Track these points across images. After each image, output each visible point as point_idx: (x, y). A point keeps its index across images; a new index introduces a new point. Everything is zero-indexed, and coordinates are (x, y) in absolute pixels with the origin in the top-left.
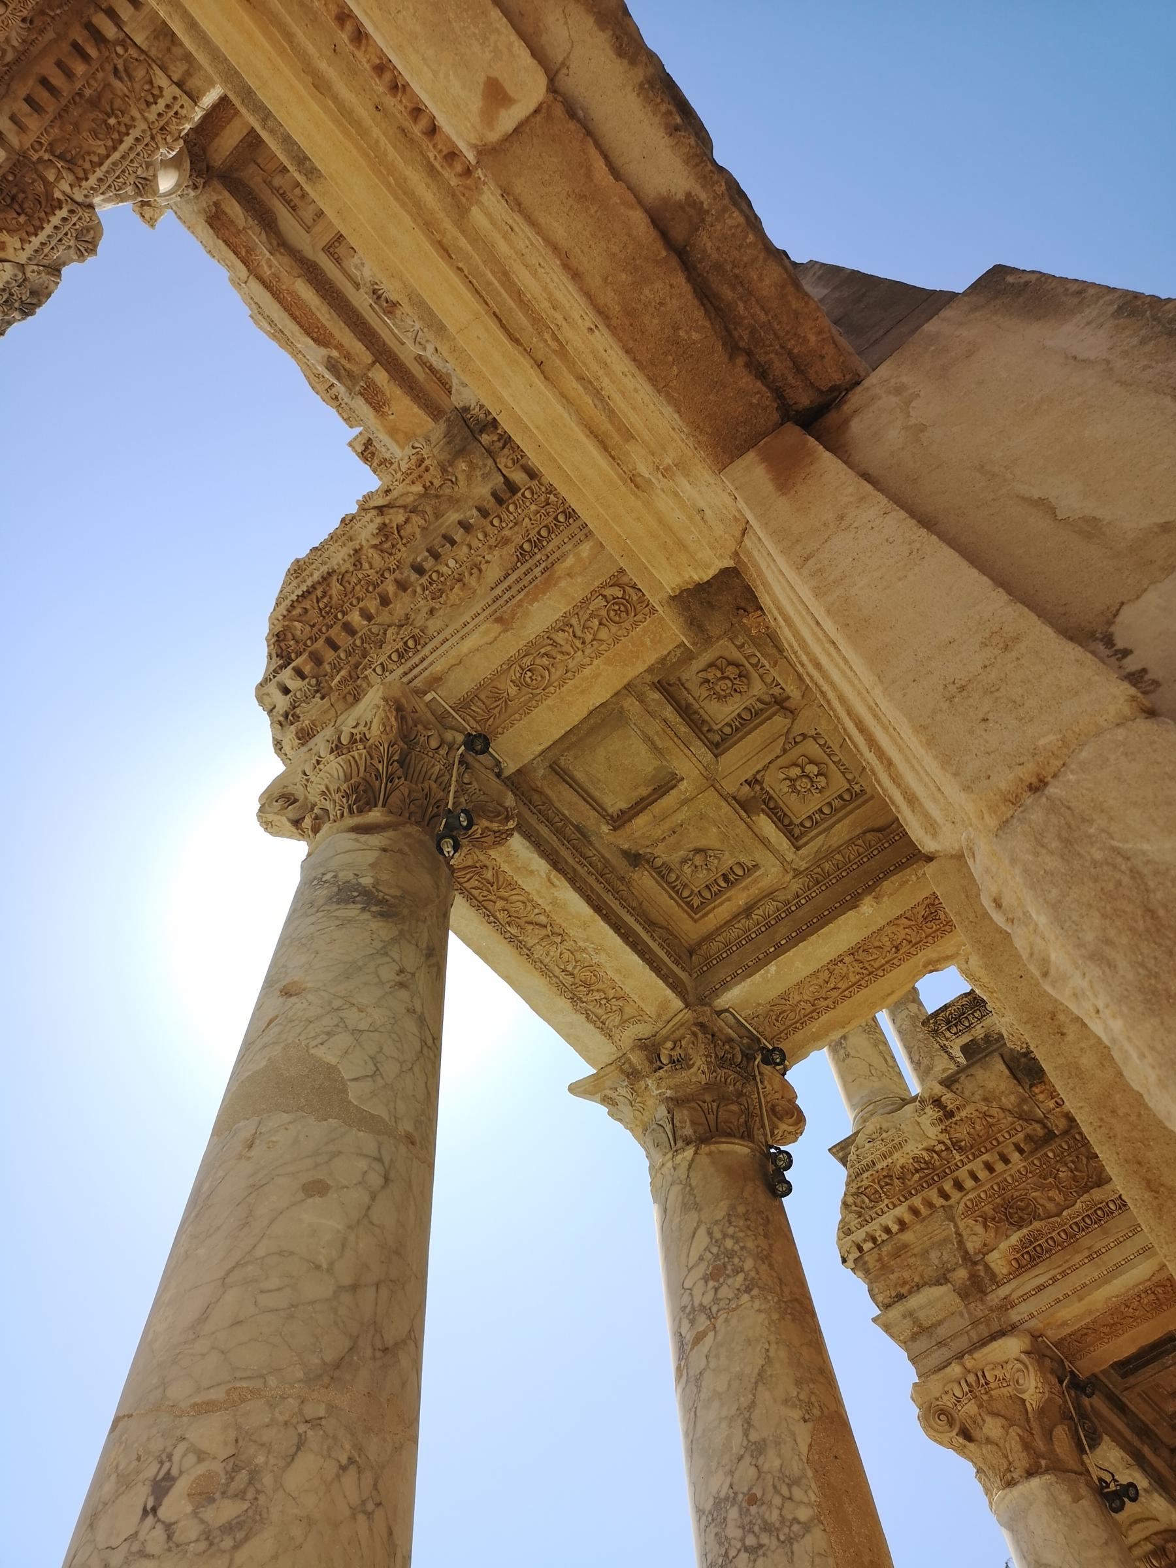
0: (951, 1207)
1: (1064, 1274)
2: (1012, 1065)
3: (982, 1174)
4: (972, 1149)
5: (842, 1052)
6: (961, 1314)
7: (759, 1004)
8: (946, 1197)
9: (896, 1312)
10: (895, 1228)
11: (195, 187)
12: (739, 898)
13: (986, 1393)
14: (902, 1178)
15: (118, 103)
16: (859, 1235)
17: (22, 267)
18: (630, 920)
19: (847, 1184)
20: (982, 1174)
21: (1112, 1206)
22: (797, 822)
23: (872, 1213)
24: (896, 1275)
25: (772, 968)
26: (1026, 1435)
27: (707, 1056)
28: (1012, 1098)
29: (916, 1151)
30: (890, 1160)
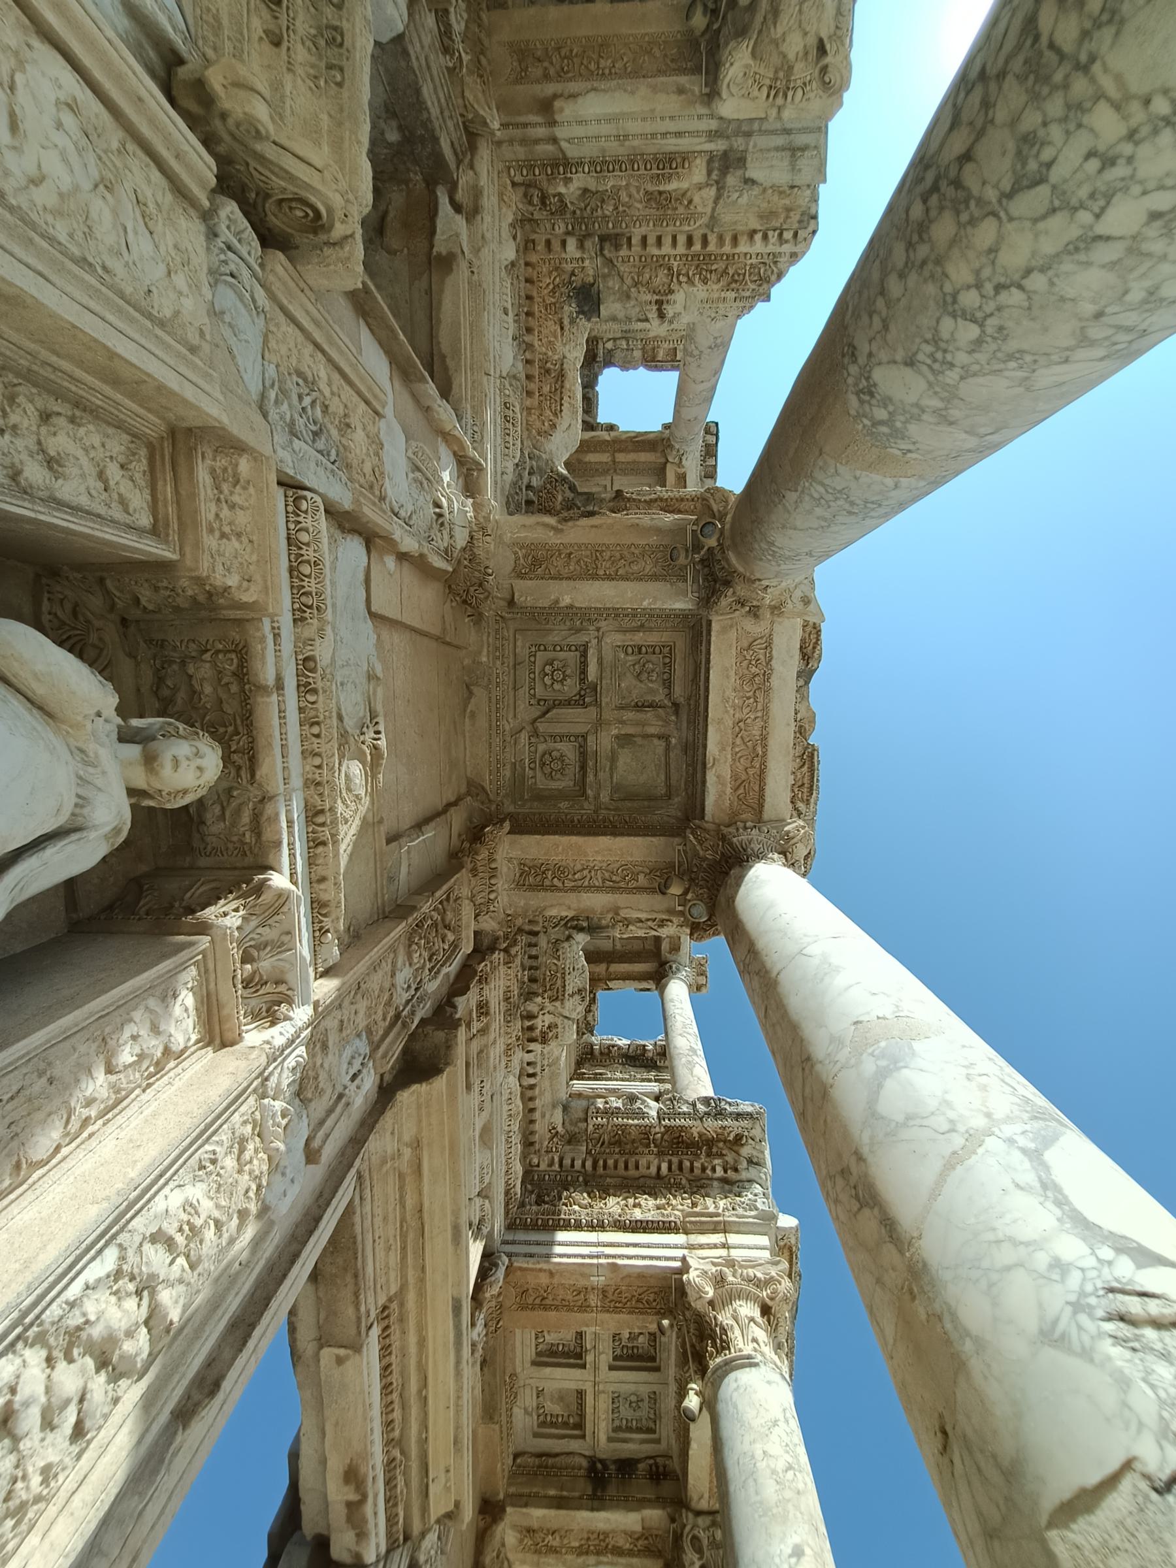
0: (707, 226)
3: (667, 241)
4: (661, 263)
5: (719, 341)
8: (705, 241)
9: (802, 179)
11: (671, 967)
12: (639, 638)
13: (777, 79)
14: (725, 272)
16: (787, 248)
17: (701, 1119)
18: (702, 684)
20: (667, 241)
22: (578, 653)
26: (770, 22)
28: (610, 284)
30: (723, 295)
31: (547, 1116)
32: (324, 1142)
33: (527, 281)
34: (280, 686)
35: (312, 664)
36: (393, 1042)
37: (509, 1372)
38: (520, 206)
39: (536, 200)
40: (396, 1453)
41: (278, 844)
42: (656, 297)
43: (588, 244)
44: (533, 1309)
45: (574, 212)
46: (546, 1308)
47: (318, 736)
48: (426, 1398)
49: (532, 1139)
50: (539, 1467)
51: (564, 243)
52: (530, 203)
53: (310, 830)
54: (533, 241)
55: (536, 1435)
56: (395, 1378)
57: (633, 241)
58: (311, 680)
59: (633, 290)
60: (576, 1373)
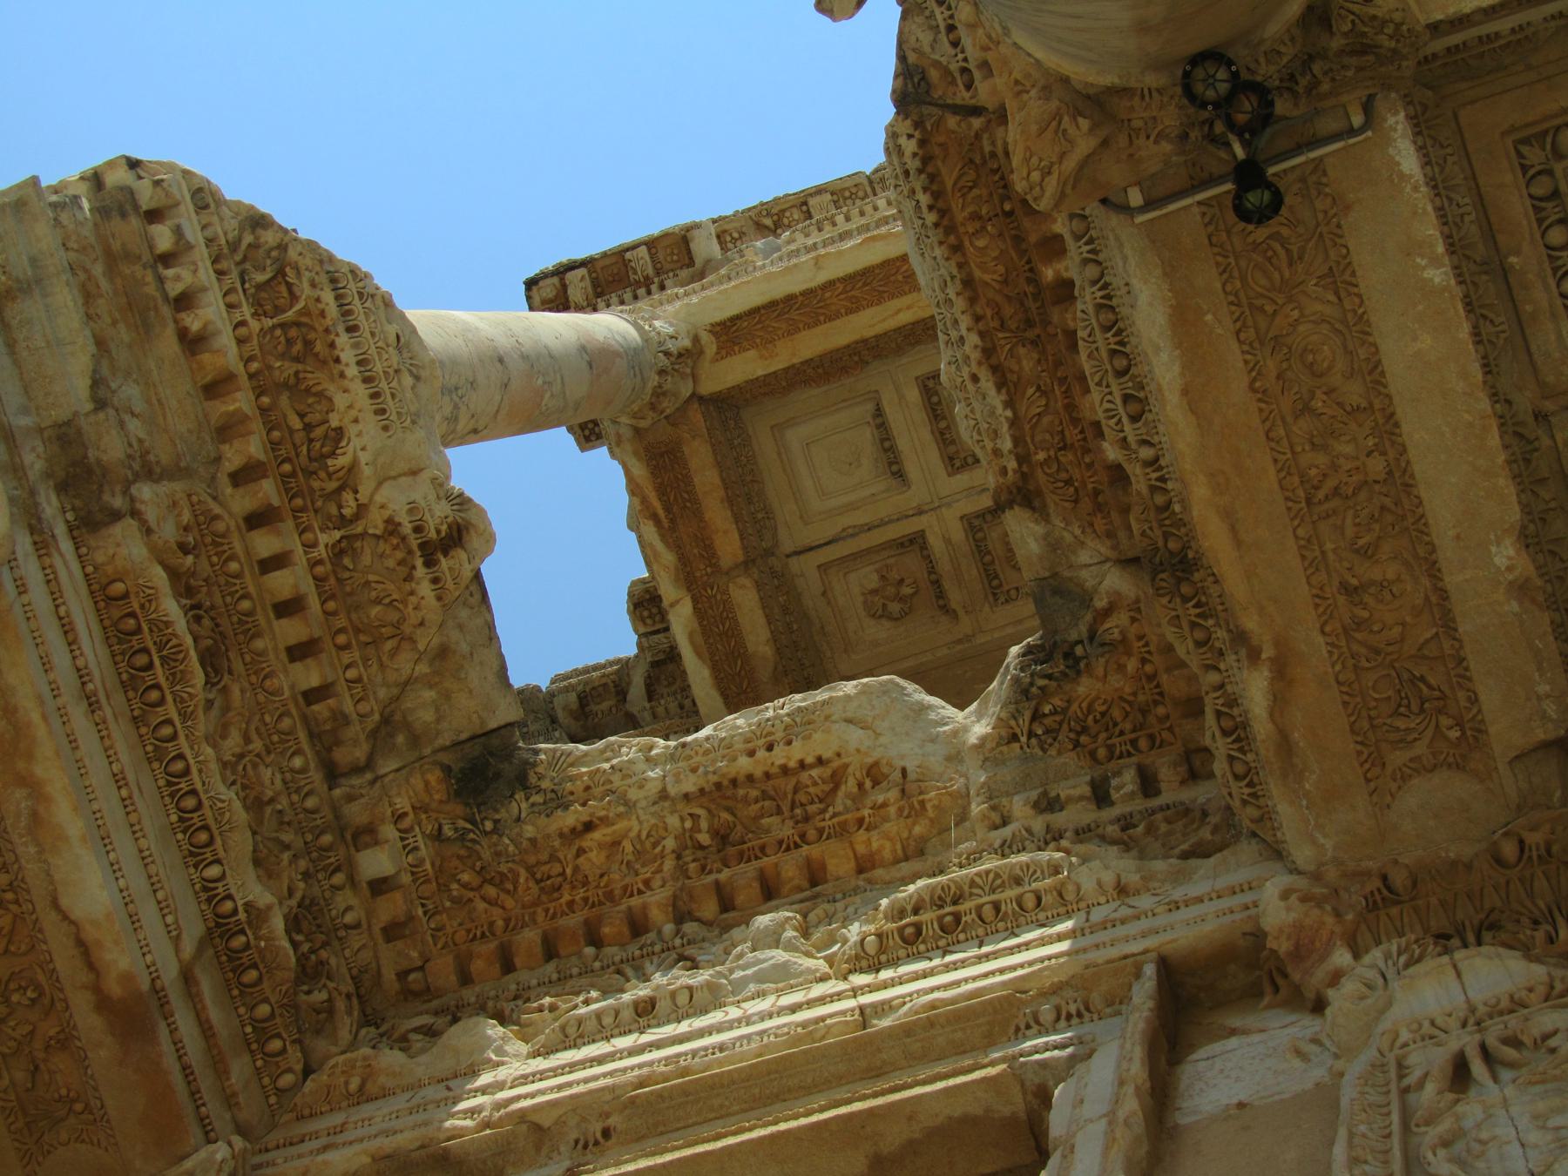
1: (93, 705)
2: (495, 741)
3: (282, 583)
6: (25, 411)
7: (1348, 208)
8: (241, 477)
10: (194, 323)
19: (312, 246)
20: (282, 583)
21: (214, 871)
23: (233, 278)
24: (104, 284)
25: (1439, 275)
27: (1398, 26)
28: (427, 716)
29: (356, 443)
30: (352, 371)
33: (508, 967)
38: (345, 1035)
39: (320, 996)
42: (421, 571)
43: (356, 813)
45: (306, 876)
51: (380, 886)
52: (329, 1009)
54: (402, 975)
57: (315, 681)
59: (421, 647)
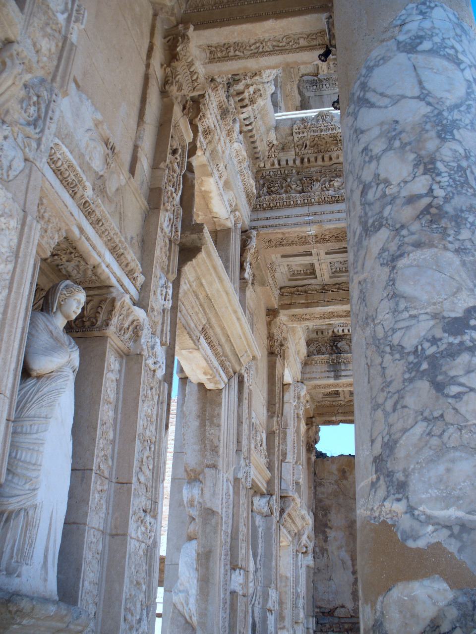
15: (311, 140)
31: (265, 139)
32: (166, 338)
34: (82, 230)
35: (87, 205)
36: (174, 259)
37: (268, 264)
40: (223, 358)
41: (109, 278)
44: (276, 246)
46: (283, 245)
47: (103, 224)
48: (230, 340)
49: (257, 156)
50: (294, 292)
53: (115, 255)
55: (290, 280)
56: (215, 341)
58: (90, 210)
60: (308, 258)
